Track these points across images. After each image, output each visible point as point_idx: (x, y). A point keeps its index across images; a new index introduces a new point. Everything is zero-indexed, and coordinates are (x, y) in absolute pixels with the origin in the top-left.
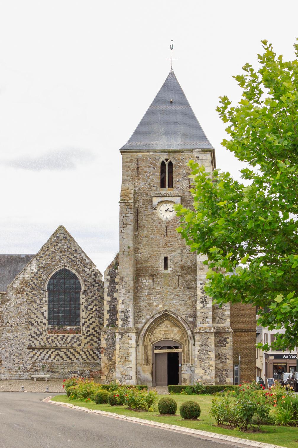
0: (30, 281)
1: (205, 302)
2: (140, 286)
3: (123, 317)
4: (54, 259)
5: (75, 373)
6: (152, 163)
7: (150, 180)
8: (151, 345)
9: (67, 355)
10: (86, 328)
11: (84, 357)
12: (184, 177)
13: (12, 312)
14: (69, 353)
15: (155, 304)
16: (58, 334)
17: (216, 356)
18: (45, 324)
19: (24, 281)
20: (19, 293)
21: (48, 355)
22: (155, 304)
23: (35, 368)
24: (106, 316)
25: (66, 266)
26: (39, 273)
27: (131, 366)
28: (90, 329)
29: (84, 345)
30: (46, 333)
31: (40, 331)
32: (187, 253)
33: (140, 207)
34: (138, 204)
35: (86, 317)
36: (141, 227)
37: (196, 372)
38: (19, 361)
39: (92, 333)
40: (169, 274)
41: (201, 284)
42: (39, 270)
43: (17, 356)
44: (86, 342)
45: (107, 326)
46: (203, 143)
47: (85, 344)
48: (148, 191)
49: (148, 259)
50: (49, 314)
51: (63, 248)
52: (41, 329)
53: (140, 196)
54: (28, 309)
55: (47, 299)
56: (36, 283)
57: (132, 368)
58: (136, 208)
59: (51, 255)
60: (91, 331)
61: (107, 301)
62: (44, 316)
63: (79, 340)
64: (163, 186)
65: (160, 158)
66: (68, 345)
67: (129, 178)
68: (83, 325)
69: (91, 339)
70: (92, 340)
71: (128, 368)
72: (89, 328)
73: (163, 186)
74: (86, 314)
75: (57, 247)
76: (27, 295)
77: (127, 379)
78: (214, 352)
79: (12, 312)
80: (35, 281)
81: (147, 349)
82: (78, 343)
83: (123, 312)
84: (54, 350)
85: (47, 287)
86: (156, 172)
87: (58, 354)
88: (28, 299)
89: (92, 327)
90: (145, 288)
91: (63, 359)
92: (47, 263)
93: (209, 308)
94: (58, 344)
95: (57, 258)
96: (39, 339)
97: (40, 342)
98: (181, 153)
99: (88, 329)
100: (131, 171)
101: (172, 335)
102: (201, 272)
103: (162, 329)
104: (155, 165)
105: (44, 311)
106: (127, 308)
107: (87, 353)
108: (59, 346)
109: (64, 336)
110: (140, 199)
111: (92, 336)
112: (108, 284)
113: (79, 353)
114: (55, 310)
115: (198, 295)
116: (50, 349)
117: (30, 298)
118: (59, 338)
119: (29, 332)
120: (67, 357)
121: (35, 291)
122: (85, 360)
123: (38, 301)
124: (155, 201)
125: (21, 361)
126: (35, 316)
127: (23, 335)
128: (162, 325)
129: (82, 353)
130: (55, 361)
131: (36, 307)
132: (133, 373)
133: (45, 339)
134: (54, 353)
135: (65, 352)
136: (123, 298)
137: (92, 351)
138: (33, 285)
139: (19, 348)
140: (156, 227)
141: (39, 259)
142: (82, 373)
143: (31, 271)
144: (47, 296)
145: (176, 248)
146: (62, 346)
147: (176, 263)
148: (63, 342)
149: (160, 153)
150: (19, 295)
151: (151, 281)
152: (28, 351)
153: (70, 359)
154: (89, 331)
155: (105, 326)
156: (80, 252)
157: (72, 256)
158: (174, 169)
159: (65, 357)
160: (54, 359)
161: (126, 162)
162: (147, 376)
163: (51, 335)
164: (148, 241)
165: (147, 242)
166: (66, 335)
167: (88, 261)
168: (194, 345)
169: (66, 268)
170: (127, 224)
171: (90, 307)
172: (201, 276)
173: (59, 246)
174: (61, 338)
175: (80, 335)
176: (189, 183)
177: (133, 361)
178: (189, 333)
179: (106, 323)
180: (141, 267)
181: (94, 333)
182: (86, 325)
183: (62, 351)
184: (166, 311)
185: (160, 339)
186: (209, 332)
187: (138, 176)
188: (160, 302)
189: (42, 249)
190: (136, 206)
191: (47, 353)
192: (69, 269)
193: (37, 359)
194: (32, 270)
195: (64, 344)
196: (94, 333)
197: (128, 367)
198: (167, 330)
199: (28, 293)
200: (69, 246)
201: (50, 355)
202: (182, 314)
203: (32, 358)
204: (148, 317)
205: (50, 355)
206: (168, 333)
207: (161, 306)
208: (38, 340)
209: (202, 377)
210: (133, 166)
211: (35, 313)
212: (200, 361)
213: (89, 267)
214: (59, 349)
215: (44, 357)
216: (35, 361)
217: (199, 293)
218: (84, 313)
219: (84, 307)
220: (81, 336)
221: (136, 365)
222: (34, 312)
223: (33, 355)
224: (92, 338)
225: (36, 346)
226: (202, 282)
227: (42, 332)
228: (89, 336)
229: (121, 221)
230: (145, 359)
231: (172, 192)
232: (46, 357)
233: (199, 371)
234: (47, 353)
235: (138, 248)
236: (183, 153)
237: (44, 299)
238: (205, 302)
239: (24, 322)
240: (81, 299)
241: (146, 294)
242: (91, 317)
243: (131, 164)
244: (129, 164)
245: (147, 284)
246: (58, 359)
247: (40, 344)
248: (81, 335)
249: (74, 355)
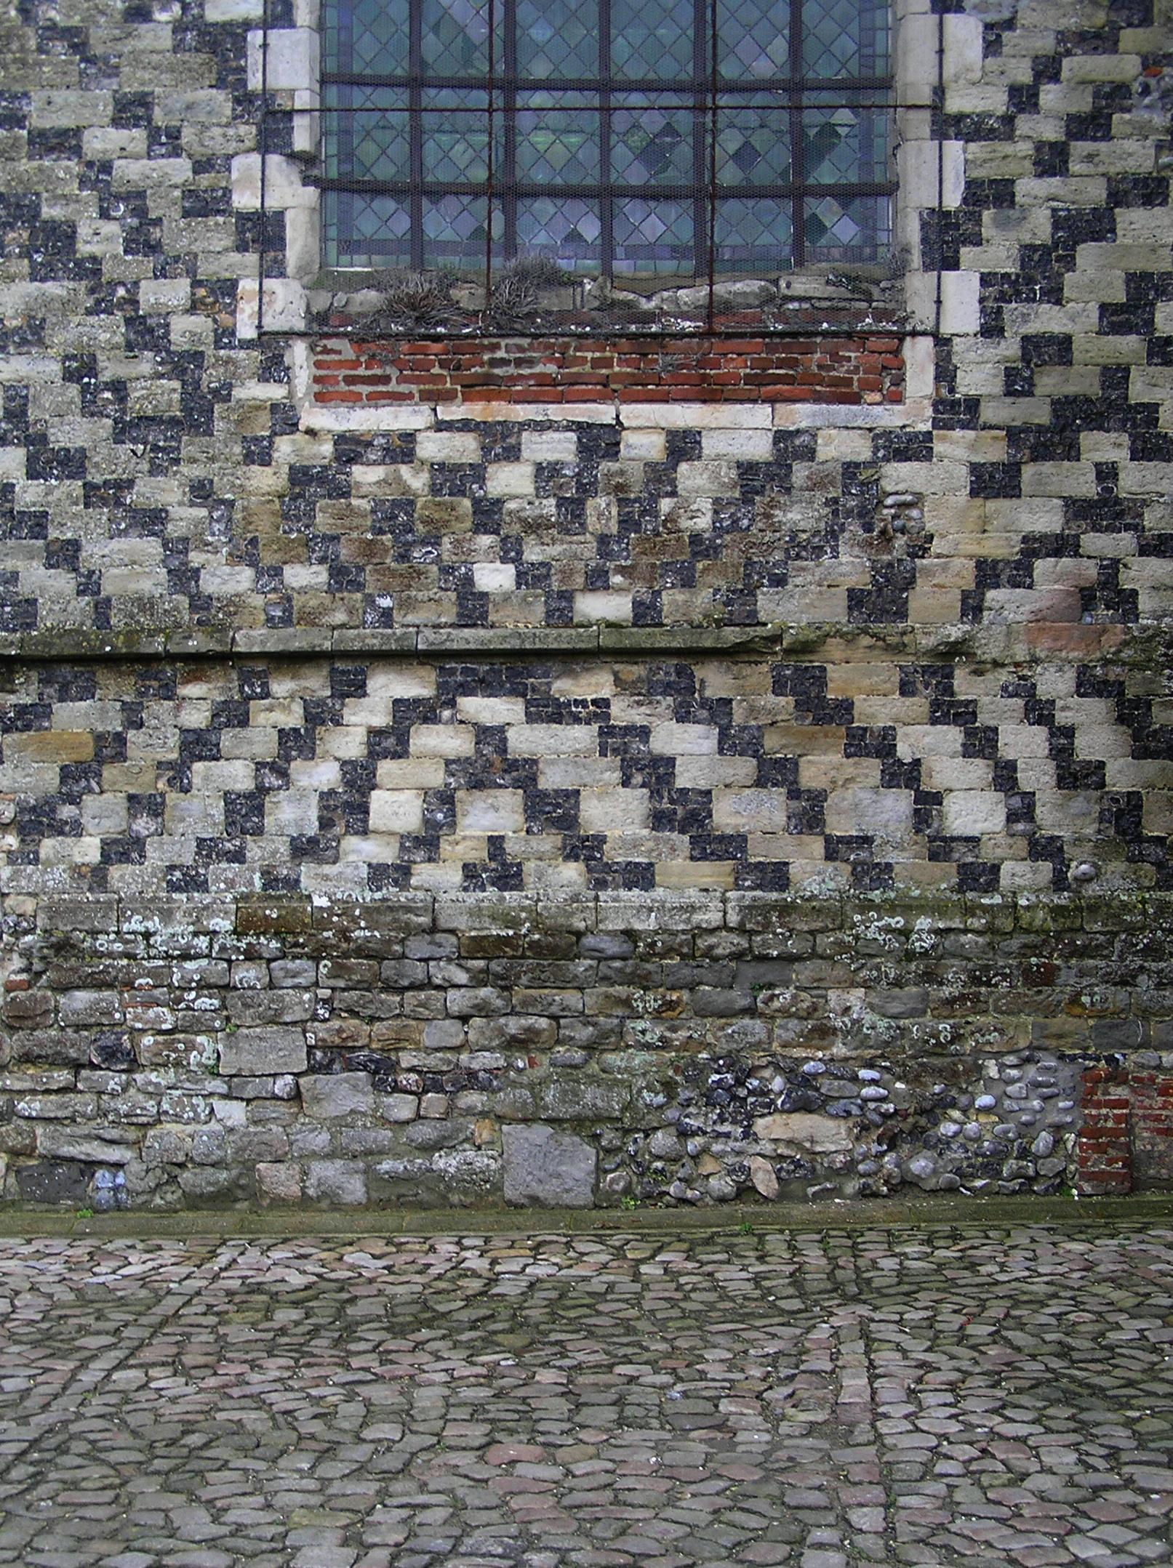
5: (806, 1097)
9: (658, 772)
10: (1000, 293)
11: (973, 812)
14: (688, 746)
16: (501, 411)
18: (262, 233)
21: (321, 775)
23: (82, 998)
28: (1070, 318)
29: (972, 607)
30: (275, 392)
31: (184, 364)
35: (997, 102)
39: (1116, 376)
44: (1000, 547)
47: (988, 573)
52: (200, 323)
60: (1096, 348)
62: (244, 99)
63: (865, 516)
66: (672, 599)
68: (946, 240)
69: (1087, 487)
70: (1104, 509)
72: (1055, 296)
74: (992, 47)
82: (850, 565)
87: (491, 765)
89: (1095, 274)
94: (494, 577)
96: (166, 491)
97: (176, 548)
99: (1048, 320)
107: (1024, 744)
108: (521, 623)
109: (599, 442)
111: (1103, 446)
113: (883, 746)
118: (510, 481)
120: (659, 820)
122: (981, 876)
126: (102, 96)
129: (933, 747)
130: (440, 877)
134: (427, 739)
135: (623, 712)
137: (1098, 708)
142: (934, 1110)
146: (560, 612)
148: (588, 549)
153: (712, 846)
159: (615, 813)
160: (427, 842)
163: (363, 420)
166: (645, 426)
174: (546, 473)
181: (1138, 391)
182: (998, 250)
183: (557, 713)
191: (297, 744)
195: (597, 581)
196: (1138, 391)
201: (360, 779)
205: (360, 779)
214: (512, 668)
215: (246, 811)
216: (98, 876)
220: (911, 447)
224: (1107, 473)
225: (102, 608)
227: (211, 378)
228: (1055, 441)
232: (292, 813)
242: (1084, 104)
246: (496, 843)
247: (183, 577)
248: (913, 410)
249: (777, 773)
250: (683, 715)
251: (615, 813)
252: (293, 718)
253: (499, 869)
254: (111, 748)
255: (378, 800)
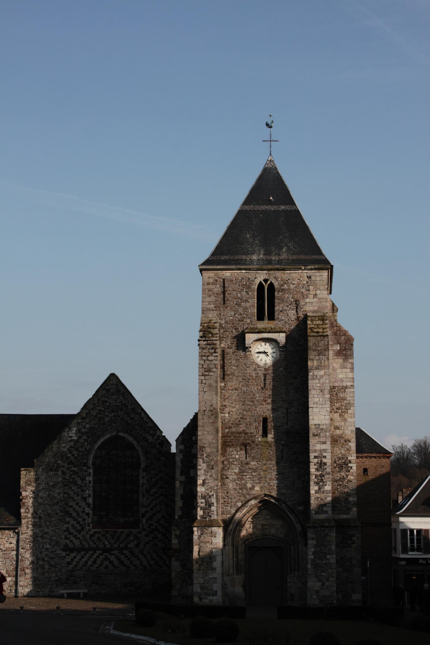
0: (68, 452)
1: (321, 484)
2: (228, 460)
3: (203, 505)
4: (102, 420)
6: (244, 285)
7: (242, 308)
8: (243, 545)
12: (290, 305)
13: (42, 498)
14: (122, 557)
15: (249, 485)
17: (337, 562)
18: (88, 514)
19: (58, 452)
20: (51, 470)
21: (92, 560)
22: (249, 485)
23: (73, 578)
24: (179, 503)
25: (120, 432)
26: (80, 441)
27: (215, 575)
30: (89, 528)
32: (295, 413)
33: (228, 348)
34: (225, 343)
36: (229, 375)
37: (309, 584)
38: (49, 569)
40: (267, 442)
41: (315, 457)
42: (80, 437)
43: (47, 561)
45: (179, 517)
46: (321, 256)
48: (238, 324)
49: (239, 421)
50: (94, 500)
51: (116, 406)
53: (227, 331)
54: (65, 493)
55: (91, 479)
56: (76, 455)
57: (216, 578)
58: (223, 348)
59: (98, 415)
61: (180, 482)
64: (260, 317)
65: (255, 278)
66: (122, 546)
67: (212, 306)
68: (143, 515)
71: (211, 578)
73: (260, 317)
74: (147, 500)
75: (107, 404)
76: (64, 473)
77: (209, 596)
78: (334, 556)
79: (42, 498)
80: (75, 452)
81: (237, 551)
82: (135, 542)
83: (203, 497)
84: (100, 552)
85: (91, 462)
86: (250, 298)
88: (65, 479)
90: (235, 463)
91: (113, 565)
92: (92, 427)
93: (327, 492)
94: (107, 543)
95: (107, 419)
96: (80, 536)
97: (81, 541)
98: (287, 272)
100: (215, 296)
101: (273, 531)
102: (316, 439)
103: (258, 522)
104: (249, 287)
105: (87, 496)
106: (210, 490)
108: (108, 546)
109: (115, 532)
110: (228, 336)
112: (182, 457)
114: (103, 494)
115: (311, 473)
116: (95, 552)
117: (67, 477)
118: (108, 536)
119: (65, 526)
121: (75, 467)
123: (79, 482)
124: (250, 338)
125: (53, 569)
127: (57, 530)
128: (260, 516)
131: (76, 490)
132: (217, 587)
133: (88, 536)
134: (101, 557)
135: (117, 554)
136: (203, 478)
138: (72, 458)
139: (50, 550)
140: (249, 376)
141: (80, 421)
143: (69, 439)
144: (92, 474)
145: (279, 405)
146: (112, 546)
147: (279, 427)
149: (256, 272)
150: (51, 473)
151: (243, 452)
152: (64, 554)
154: (152, 525)
155: (177, 517)
156: (140, 411)
157: (128, 417)
158: (276, 293)
159: (116, 562)
160: (101, 565)
161: (208, 284)
162: (239, 590)
163: (95, 530)
164: (238, 395)
165: (238, 397)
167: (150, 424)
168: (306, 545)
169: (119, 434)
170: (209, 370)
171: (154, 490)
172: (315, 446)
173: (110, 403)
175: (138, 530)
176: (297, 314)
177: (218, 569)
178: (298, 527)
179: (178, 513)
180: (228, 433)
184: (266, 495)
185: (256, 537)
186: (328, 527)
187: (224, 304)
188: (257, 483)
189: (85, 407)
190: (222, 345)
191: (91, 557)
192: (124, 435)
193: (76, 566)
194: (71, 437)
195: (115, 544)
197: (211, 577)
198: (266, 523)
199: (65, 470)
200: (124, 402)
202: (287, 500)
203: (69, 563)
204: (239, 504)
205: (96, 560)
206: (267, 527)
207: (257, 488)
208: (79, 538)
209: (317, 592)
210: (218, 289)
211: (75, 498)
212: (315, 568)
213: (151, 432)
217: (313, 469)
218: (145, 498)
219: (144, 491)
220: (140, 533)
221: (222, 574)
222: (73, 498)
223: (70, 560)
225: (74, 546)
226: (316, 454)
227: (84, 526)
229: (201, 366)
230: (235, 565)
231: (273, 327)
232: (90, 563)
233: (313, 584)
234: (91, 557)
235: (225, 406)
236: (289, 272)
237: (87, 478)
238: (321, 484)
239: (58, 512)
240: (141, 478)
241: (237, 471)
243: (215, 286)
244: (211, 287)
245: (237, 457)
246: (106, 565)
247: (81, 543)
249: (129, 559)
250: (122, 555)
251: (116, 562)
252: (90, 555)
253: (107, 567)
254: (75, 557)
255: (97, 561)
